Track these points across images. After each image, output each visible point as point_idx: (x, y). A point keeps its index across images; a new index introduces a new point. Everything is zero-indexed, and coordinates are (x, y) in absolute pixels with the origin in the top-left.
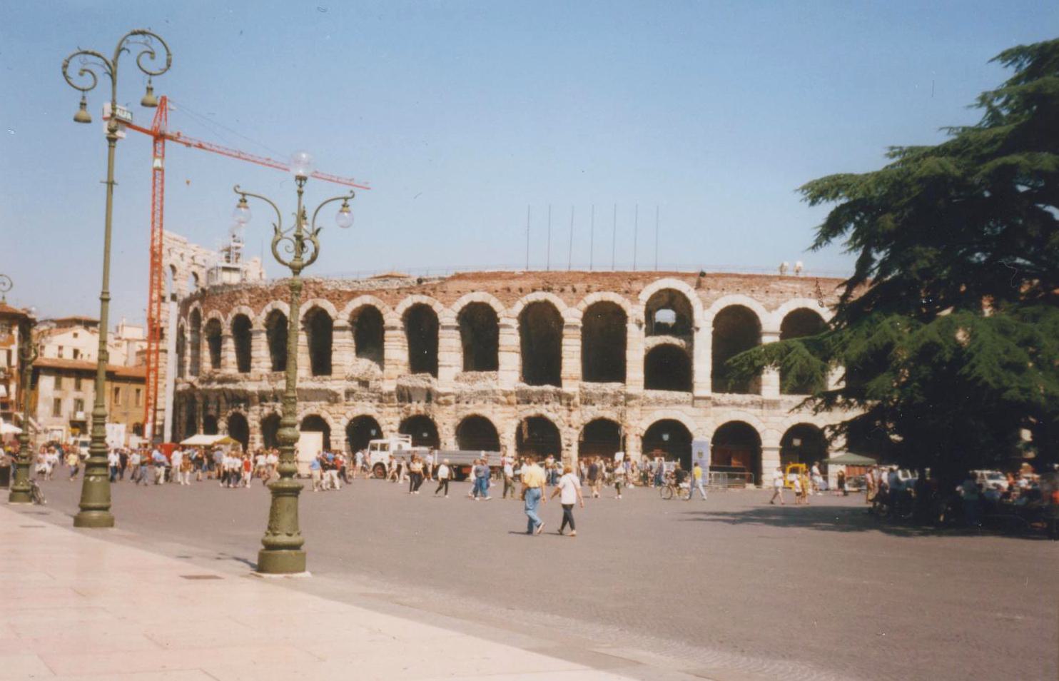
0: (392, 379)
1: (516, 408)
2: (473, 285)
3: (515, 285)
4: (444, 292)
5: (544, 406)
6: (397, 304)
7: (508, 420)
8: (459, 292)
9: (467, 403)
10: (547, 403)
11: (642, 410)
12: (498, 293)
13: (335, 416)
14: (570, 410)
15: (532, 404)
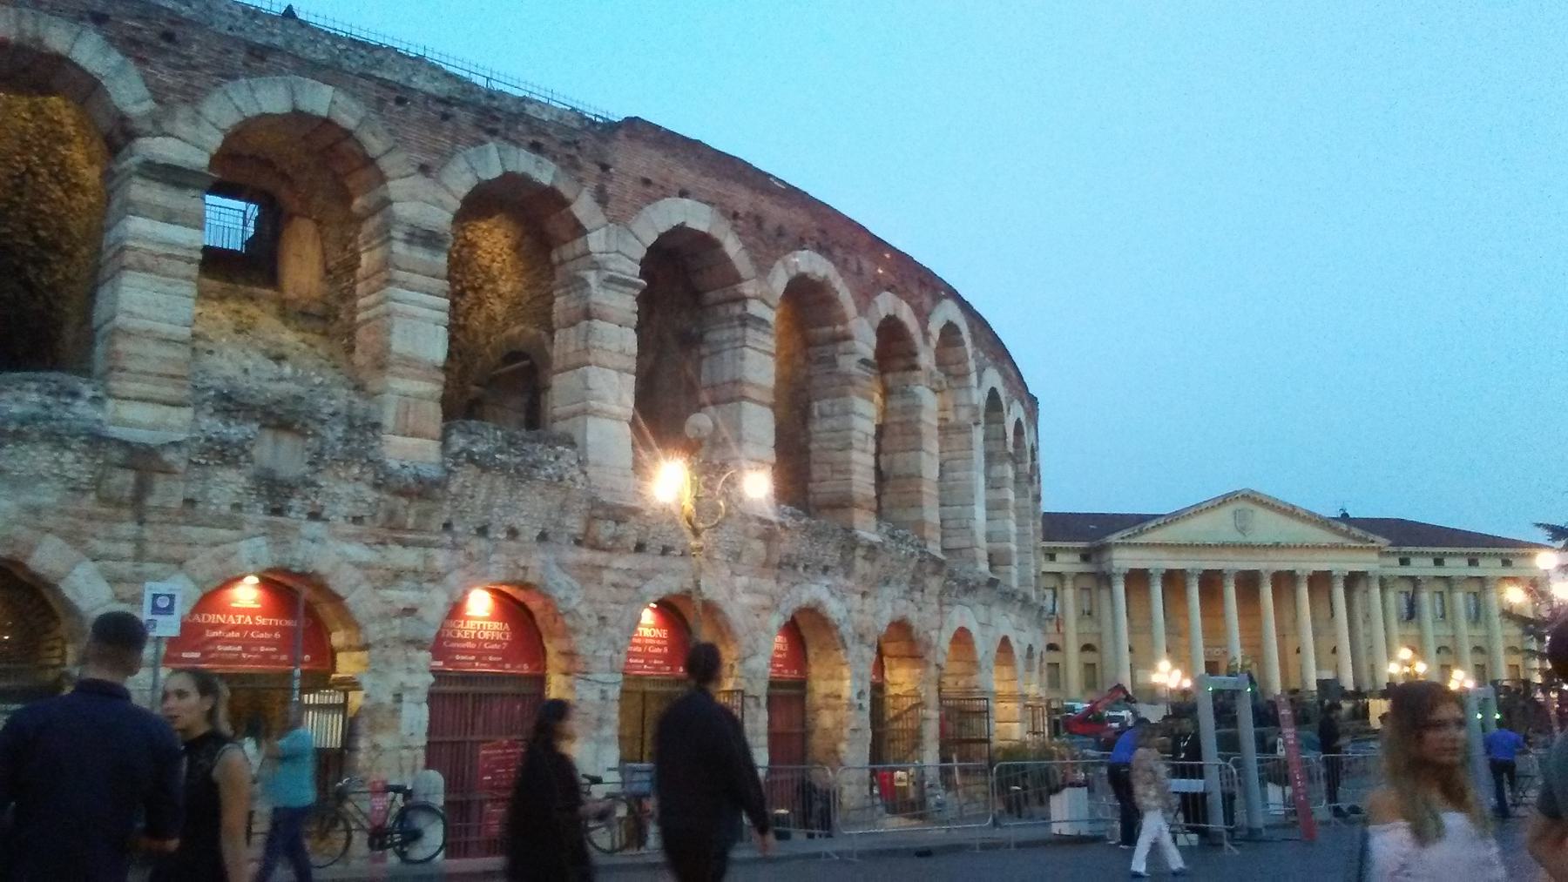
0: (413, 435)
1: (778, 580)
2: (684, 175)
3: (776, 214)
4: (605, 167)
5: (827, 582)
6: (446, 157)
7: (764, 616)
8: (647, 182)
9: (665, 551)
10: (826, 569)
11: (941, 604)
12: (740, 222)
13: (126, 568)
14: (864, 594)
15: (801, 569)
